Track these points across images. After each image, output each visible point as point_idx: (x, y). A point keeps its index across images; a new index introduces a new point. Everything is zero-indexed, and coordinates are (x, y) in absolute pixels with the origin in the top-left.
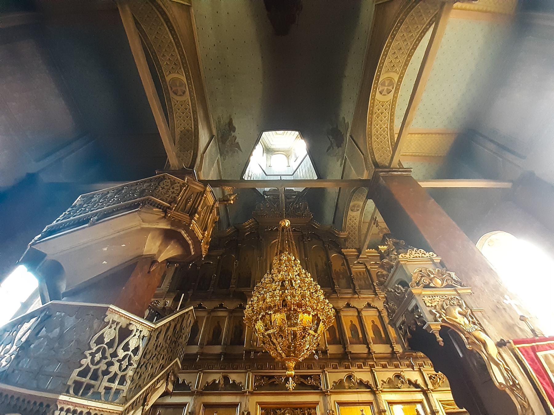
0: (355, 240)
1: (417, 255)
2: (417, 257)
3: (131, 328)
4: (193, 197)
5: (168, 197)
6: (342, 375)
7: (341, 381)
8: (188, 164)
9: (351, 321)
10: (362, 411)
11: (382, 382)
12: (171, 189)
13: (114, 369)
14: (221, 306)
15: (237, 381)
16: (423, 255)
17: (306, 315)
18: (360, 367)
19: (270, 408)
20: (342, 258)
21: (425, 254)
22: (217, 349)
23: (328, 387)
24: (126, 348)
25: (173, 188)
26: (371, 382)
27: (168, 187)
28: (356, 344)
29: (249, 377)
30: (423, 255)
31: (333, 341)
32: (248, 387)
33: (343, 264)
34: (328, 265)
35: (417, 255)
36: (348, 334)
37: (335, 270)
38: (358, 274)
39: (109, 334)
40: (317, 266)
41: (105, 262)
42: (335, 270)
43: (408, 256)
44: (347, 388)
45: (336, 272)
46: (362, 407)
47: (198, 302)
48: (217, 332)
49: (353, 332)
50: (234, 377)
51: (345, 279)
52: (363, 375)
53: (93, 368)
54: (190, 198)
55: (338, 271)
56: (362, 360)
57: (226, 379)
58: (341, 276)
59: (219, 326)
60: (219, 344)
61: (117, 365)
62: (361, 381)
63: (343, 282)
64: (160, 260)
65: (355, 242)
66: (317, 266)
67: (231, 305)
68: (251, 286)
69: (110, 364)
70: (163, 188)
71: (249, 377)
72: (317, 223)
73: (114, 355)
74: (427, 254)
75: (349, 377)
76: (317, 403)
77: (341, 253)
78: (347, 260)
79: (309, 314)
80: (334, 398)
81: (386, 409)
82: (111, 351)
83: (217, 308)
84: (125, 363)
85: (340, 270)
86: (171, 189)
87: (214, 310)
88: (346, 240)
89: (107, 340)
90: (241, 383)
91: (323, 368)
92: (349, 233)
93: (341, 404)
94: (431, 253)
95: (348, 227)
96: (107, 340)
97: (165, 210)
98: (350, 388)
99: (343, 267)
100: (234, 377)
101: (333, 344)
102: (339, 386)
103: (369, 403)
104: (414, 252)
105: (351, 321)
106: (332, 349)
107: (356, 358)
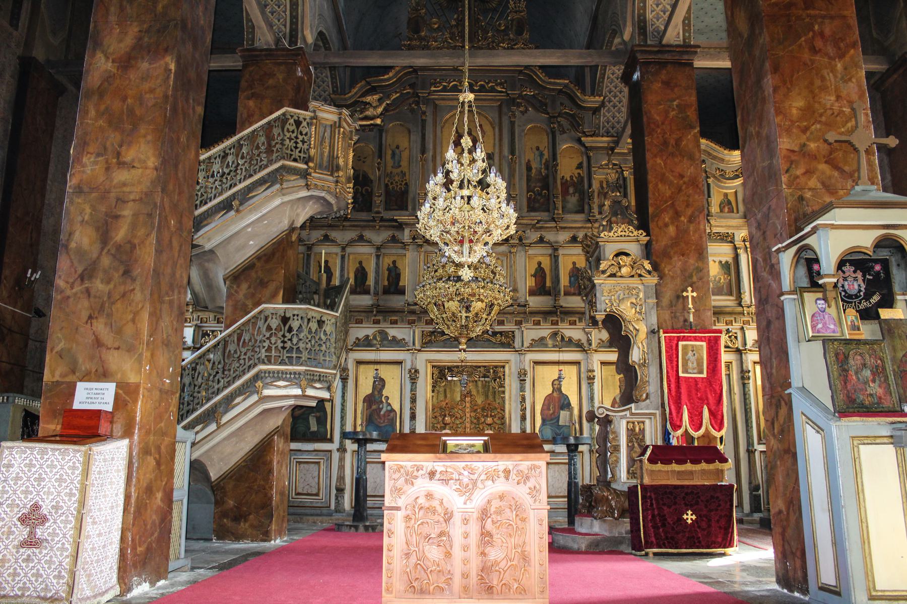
0: (619, 105)
1: (623, 233)
2: (621, 236)
3: (324, 319)
4: (327, 135)
5: (300, 152)
6: (545, 331)
7: (542, 339)
8: (286, 22)
9: (574, 263)
10: (561, 370)
11: (599, 341)
12: (299, 136)
13: (323, 348)
14: (361, 238)
15: (399, 336)
16: (630, 234)
17: (480, 303)
18: (573, 323)
19: (445, 366)
20: (582, 153)
21: (632, 233)
22: (365, 300)
23: (523, 345)
24: (325, 334)
25: (301, 134)
26: (584, 341)
27: (295, 134)
28: (574, 294)
29: (414, 332)
30: (630, 234)
31: (540, 290)
32: (414, 344)
33: (580, 166)
34: (552, 164)
35: (623, 233)
36: (564, 281)
37: (563, 177)
38: (605, 186)
39: (314, 326)
40: (529, 168)
41: (251, 243)
42: (563, 177)
43: (611, 234)
44: (550, 346)
45: (564, 181)
46: (561, 367)
47: (323, 232)
48: (361, 274)
49: (572, 279)
50: (393, 332)
51: (577, 195)
52: (574, 333)
53: (313, 349)
54: (323, 138)
55: (569, 179)
56: (577, 315)
57: (383, 334)
58: (571, 190)
59: (363, 269)
60: (367, 292)
61: (324, 346)
62: (570, 340)
63: (573, 200)
64: (299, 225)
65: (619, 108)
66: (529, 168)
67: (379, 237)
68: (410, 208)
69: (320, 345)
70: (290, 139)
71: (414, 332)
72: (541, 73)
73: (320, 339)
74: (635, 233)
75: (555, 335)
76: (507, 362)
77: (579, 141)
78: (589, 158)
79: (482, 301)
80: (531, 357)
81: (595, 368)
82: (317, 338)
83: (355, 241)
84: (328, 344)
85: (571, 177)
86: (299, 136)
87: (351, 243)
88: (596, 111)
89: (313, 330)
90: (404, 339)
91: (519, 323)
92: (603, 104)
93: (537, 363)
94: (640, 232)
95: (608, 78)
96: (313, 330)
97: (305, 175)
98: (554, 346)
99: (579, 171)
100: (393, 332)
101: (540, 294)
102: (539, 343)
103: (577, 363)
104: (620, 230)
105: (574, 263)
106: (535, 302)
107: (567, 313)
